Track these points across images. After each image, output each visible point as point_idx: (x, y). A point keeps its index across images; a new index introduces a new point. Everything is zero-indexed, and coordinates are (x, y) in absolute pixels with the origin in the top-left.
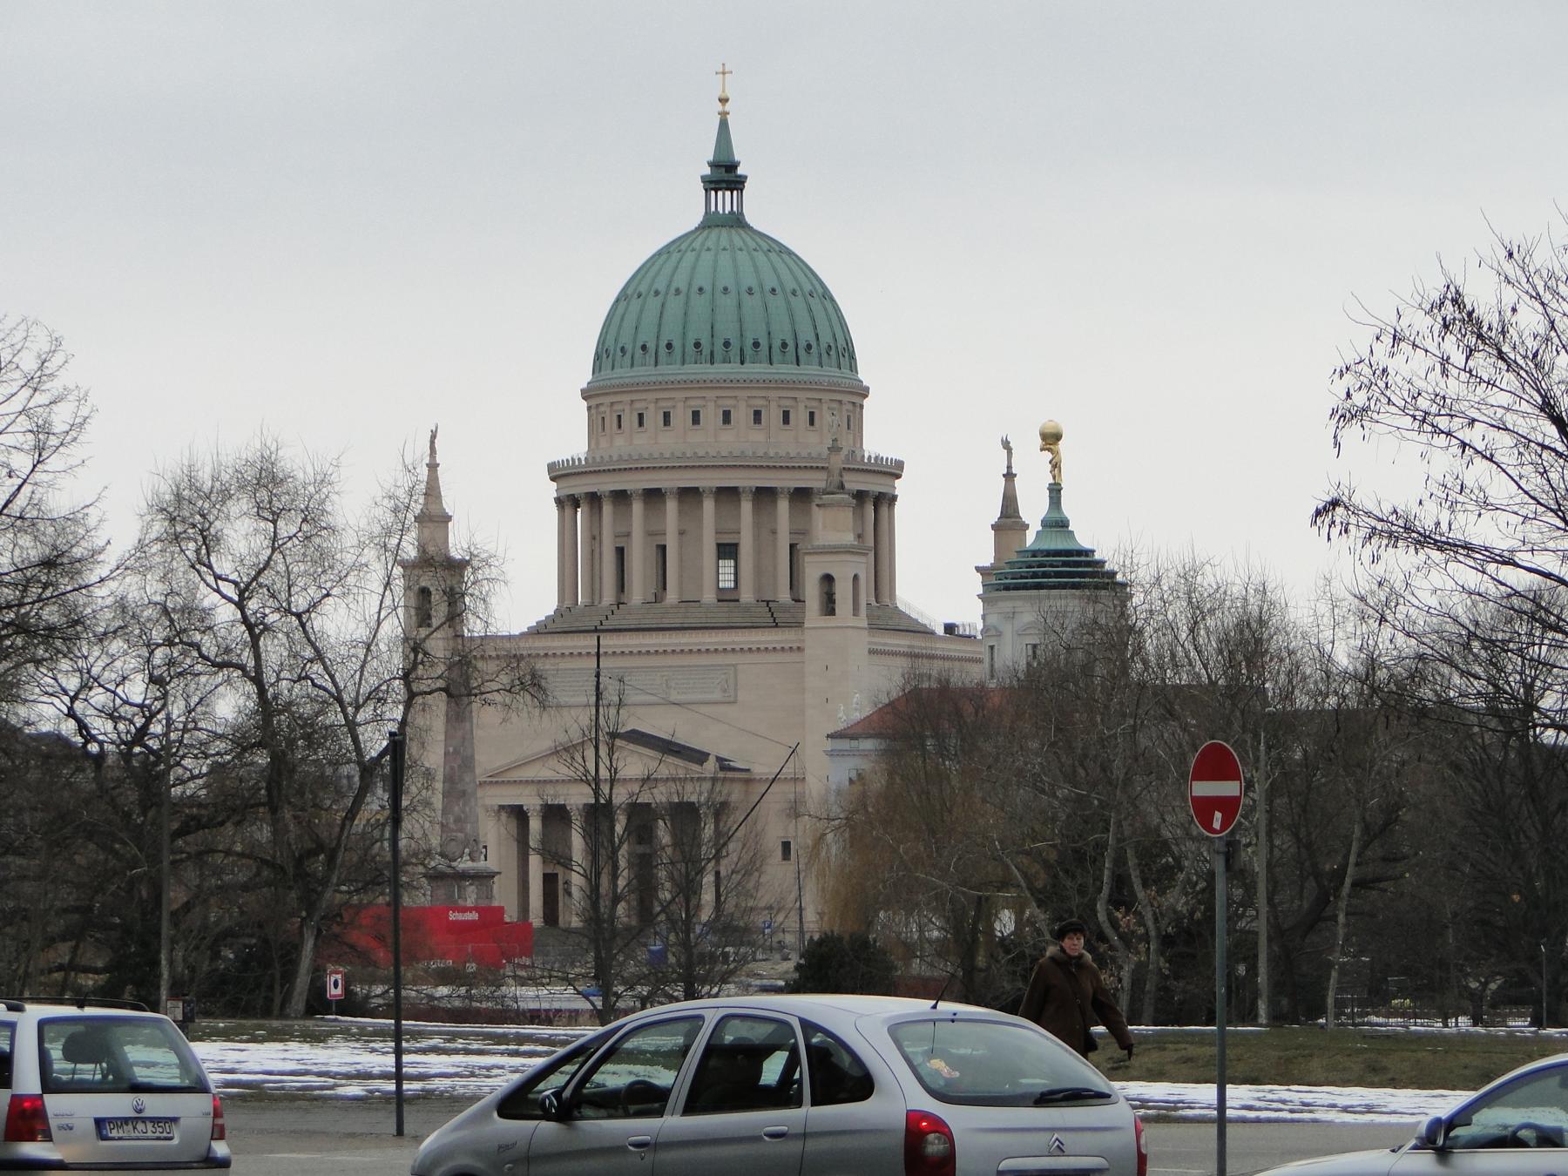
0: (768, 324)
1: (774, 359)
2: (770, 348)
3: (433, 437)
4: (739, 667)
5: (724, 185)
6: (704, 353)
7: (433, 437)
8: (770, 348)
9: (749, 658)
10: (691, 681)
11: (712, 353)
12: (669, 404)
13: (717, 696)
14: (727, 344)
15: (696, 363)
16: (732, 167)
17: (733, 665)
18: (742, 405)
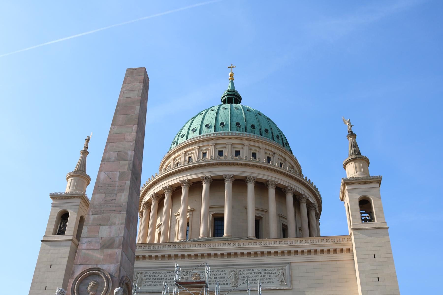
0: (270, 126)
1: (275, 139)
2: (273, 134)
3: (88, 140)
4: (293, 264)
5: (234, 97)
6: (241, 127)
7: (88, 140)
8: (273, 134)
9: (300, 258)
10: (254, 275)
11: (246, 128)
12: (225, 146)
13: (276, 285)
14: (253, 126)
15: (237, 131)
16: (236, 92)
17: (288, 263)
18: (262, 151)
